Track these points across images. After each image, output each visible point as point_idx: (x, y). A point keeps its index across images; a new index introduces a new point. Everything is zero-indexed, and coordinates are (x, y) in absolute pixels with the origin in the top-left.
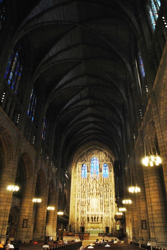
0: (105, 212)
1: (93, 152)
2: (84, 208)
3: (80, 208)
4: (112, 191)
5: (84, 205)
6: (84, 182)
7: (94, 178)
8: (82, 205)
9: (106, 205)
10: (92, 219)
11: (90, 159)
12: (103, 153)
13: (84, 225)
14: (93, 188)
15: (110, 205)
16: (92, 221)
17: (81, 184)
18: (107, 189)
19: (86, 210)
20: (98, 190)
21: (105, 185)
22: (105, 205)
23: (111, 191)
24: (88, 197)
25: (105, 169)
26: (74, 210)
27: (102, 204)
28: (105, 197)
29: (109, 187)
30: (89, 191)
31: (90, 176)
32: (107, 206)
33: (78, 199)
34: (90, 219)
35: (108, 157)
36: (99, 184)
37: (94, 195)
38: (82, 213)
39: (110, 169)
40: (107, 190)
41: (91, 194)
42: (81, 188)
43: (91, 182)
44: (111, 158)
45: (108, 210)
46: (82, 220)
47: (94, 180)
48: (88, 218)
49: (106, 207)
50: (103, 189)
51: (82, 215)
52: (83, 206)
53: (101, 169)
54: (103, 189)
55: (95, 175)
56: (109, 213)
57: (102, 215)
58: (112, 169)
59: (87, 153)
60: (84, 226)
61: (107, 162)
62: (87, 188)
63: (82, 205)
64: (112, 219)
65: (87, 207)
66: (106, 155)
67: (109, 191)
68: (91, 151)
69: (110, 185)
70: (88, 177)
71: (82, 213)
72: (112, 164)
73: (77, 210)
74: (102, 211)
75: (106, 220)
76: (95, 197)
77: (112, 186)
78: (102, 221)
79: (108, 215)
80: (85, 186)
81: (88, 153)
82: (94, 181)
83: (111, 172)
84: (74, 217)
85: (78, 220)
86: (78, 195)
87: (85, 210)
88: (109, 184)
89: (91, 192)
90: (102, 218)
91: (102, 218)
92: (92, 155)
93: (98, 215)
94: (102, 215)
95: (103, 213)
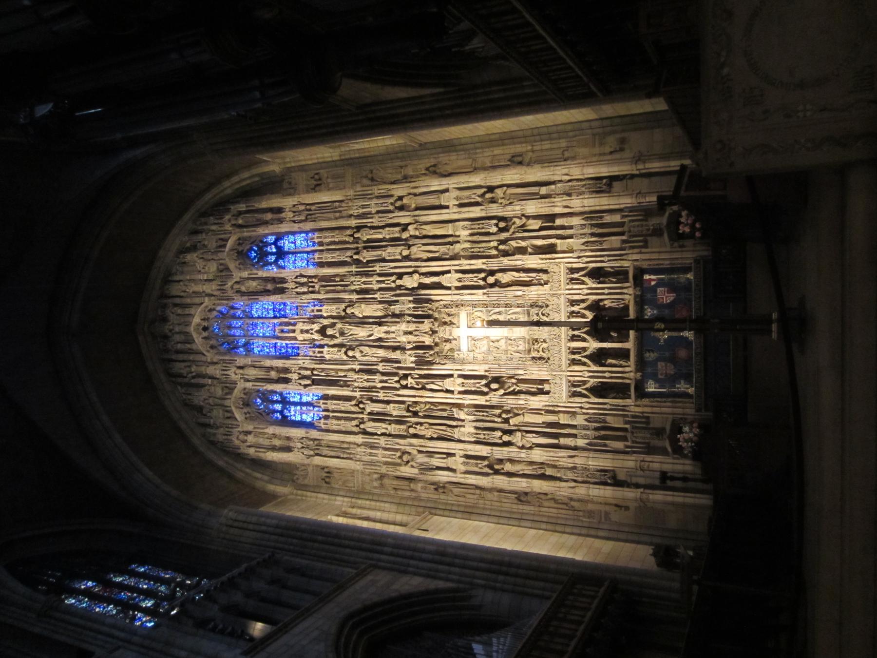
0: (551, 249)
1: (177, 338)
2: (529, 418)
3: (523, 454)
4: (400, 198)
5: (506, 421)
6: (347, 416)
7: (316, 336)
8: (506, 438)
9: (503, 242)
10: (610, 361)
11: (216, 363)
12: (186, 269)
13: (656, 423)
14: (379, 343)
15: (495, 210)
16: (623, 354)
17: (359, 439)
18: (386, 234)
19: (537, 402)
20: (396, 309)
21: (366, 256)
22: (501, 247)
23: (398, 204)
24: (448, 384)
25: (281, 254)
26: (546, 504)
27: (492, 273)
28: (443, 249)
29: (375, 221)
30: (405, 377)
31: (308, 364)
32: (504, 235)
33: (457, 462)
34: (607, 373)
35: (196, 232)
36: (354, 297)
37: (428, 340)
38: (563, 441)
39: (269, 216)
40: (395, 232)
41: (421, 362)
42: (382, 441)
43: (343, 362)
44: (204, 214)
45: (535, 224)
46: (619, 445)
47: (332, 337)
48: (600, 390)
49: (514, 244)
50: (388, 267)
51: (581, 442)
52: (510, 432)
53: (270, 287)
54: (388, 267)
55: (300, 326)
56: (563, 215)
57: (578, 270)
58: (264, 205)
59: (186, 380)
60: (668, 428)
61: (229, 244)
62: (381, 395)
63: (506, 438)
64: (610, 185)
65: (514, 393)
66: (194, 248)
67: (404, 218)
68: (174, 357)
69: (358, 217)
70: (315, 383)
71: (563, 441)
72: (234, 203)
73: (543, 477)
74: (545, 277)
75: (615, 241)
76: (444, 332)
77: (364, 196)
78: (620, 275)
79: (576, 221)
80: (371, 407)
81: (181, 376)
82: (337, 335)
83: (280, 210)
84: (607, 508)
85: (621, 476)
86: (436, 462)
87: (536, 411)
88: (353, 222)
89: (409, 359)
90: (597, 274)
91: (597, 274)
92: (194, 347)
93: (573, 303)
94: (572, 271)
95: (559, 265)
